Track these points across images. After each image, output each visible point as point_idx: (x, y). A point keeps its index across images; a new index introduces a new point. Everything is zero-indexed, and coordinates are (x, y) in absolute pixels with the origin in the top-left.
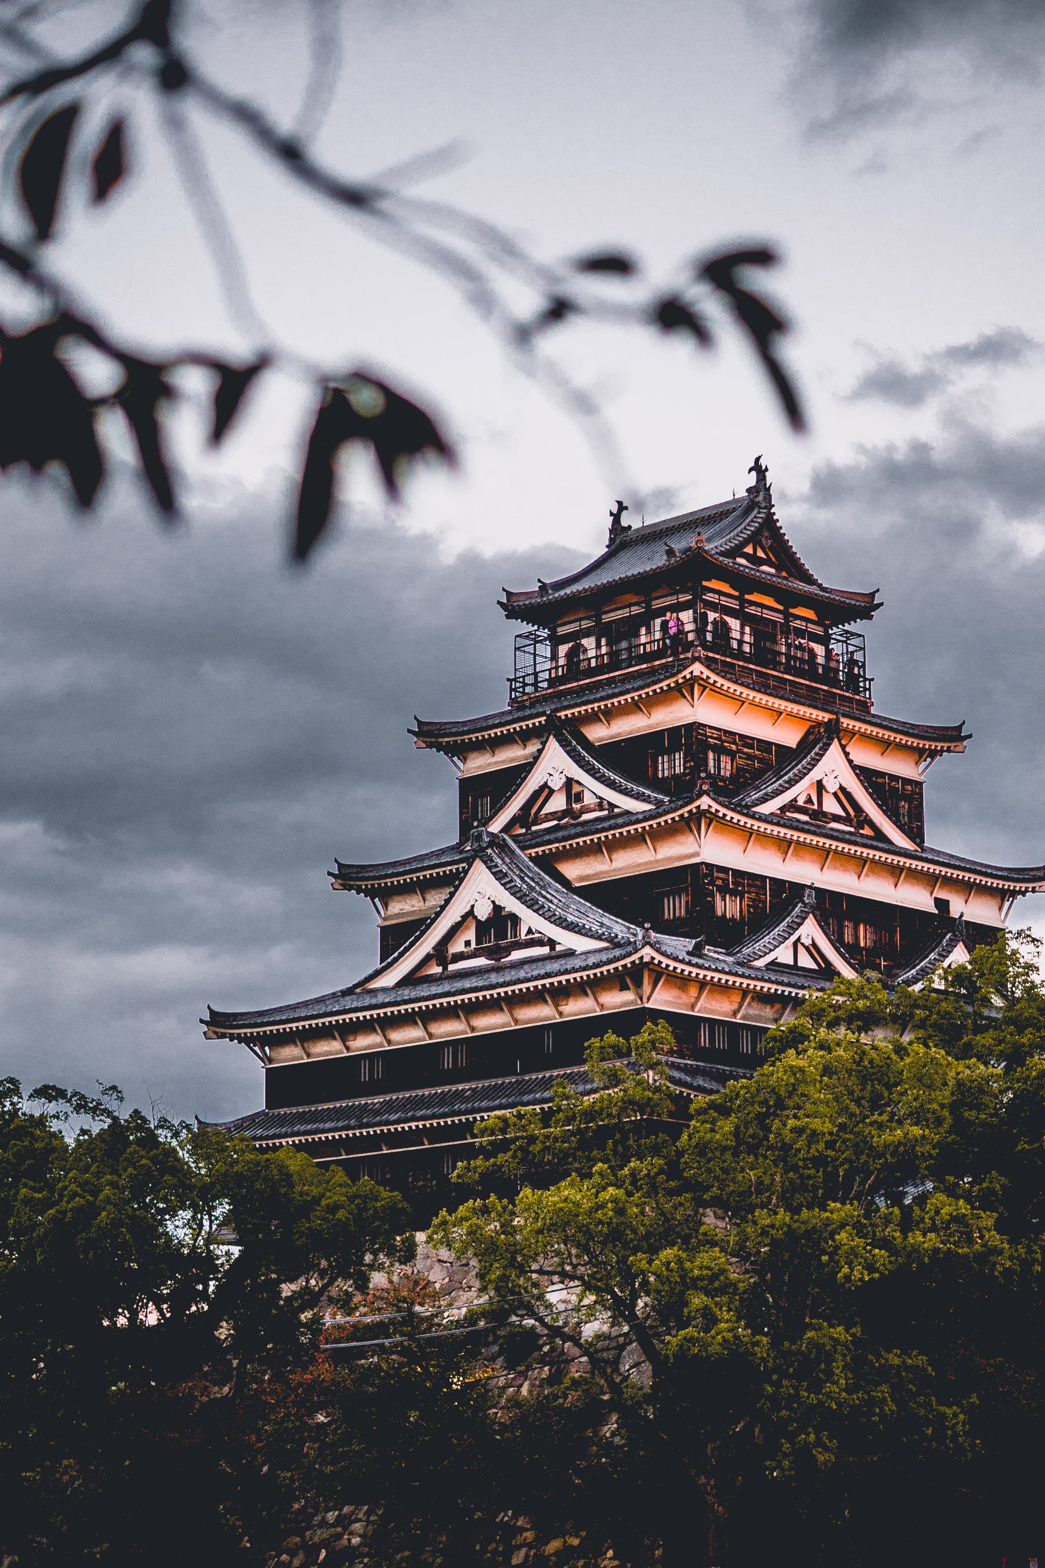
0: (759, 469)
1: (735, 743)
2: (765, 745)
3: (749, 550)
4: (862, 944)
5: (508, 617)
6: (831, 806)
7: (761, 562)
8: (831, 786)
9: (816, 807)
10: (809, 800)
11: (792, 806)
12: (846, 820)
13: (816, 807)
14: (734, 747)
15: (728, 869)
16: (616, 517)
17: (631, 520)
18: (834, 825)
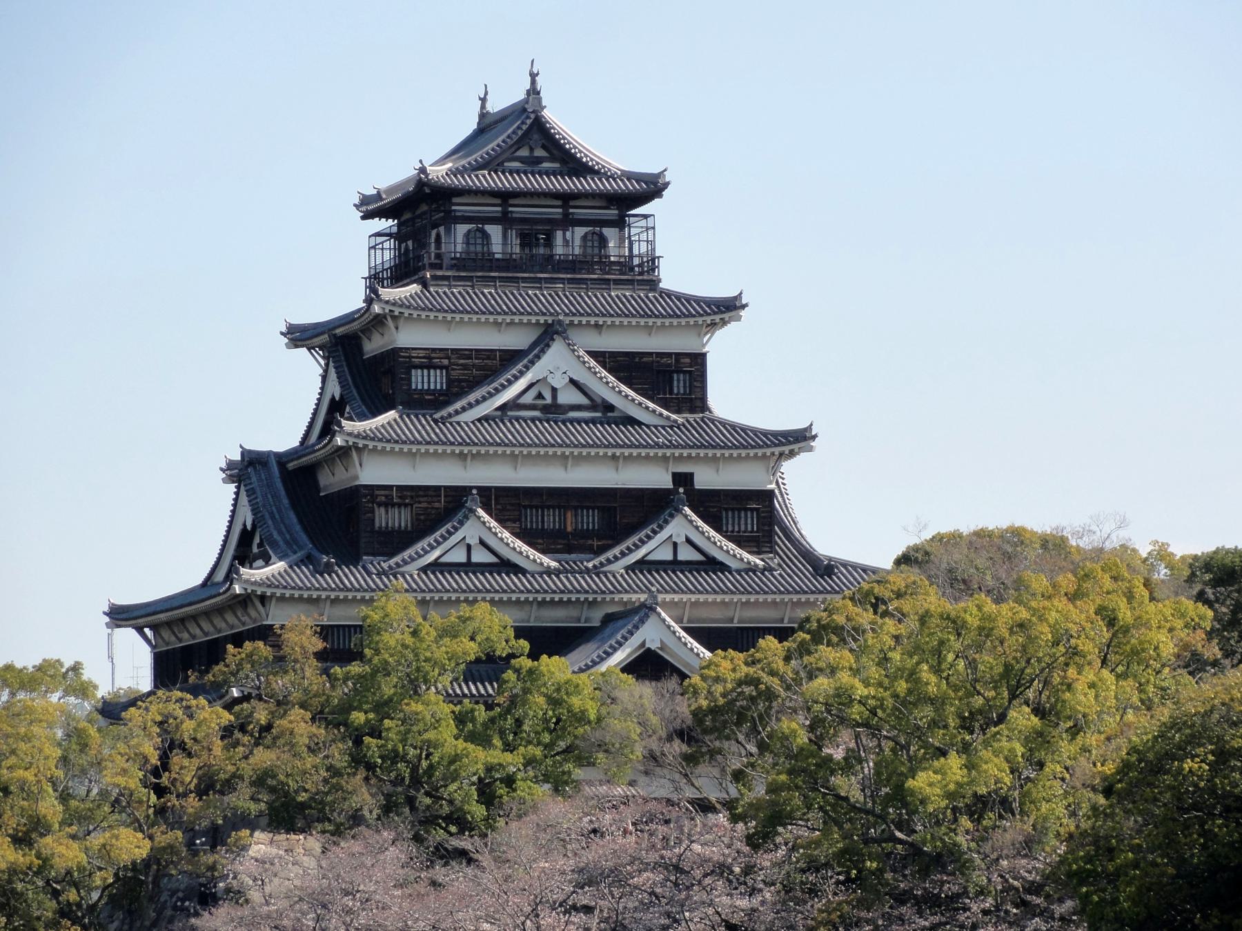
0: (533, 76)
1: (449, 358)
2: (489, 354)
3: (524, 152)
4: (569, 529)
5: (364, 218)
6: (569, 397)
7: (539, 161)
8: (559, 381)
9: (549, 400)
10: (540, 396)
11: (513, 405)
12: (593, 407)
13: (549, 400)
14: (446, 362)
15: (391, 487)
16: (483, 100)
17: (495, 106)
18: (573, 414)
